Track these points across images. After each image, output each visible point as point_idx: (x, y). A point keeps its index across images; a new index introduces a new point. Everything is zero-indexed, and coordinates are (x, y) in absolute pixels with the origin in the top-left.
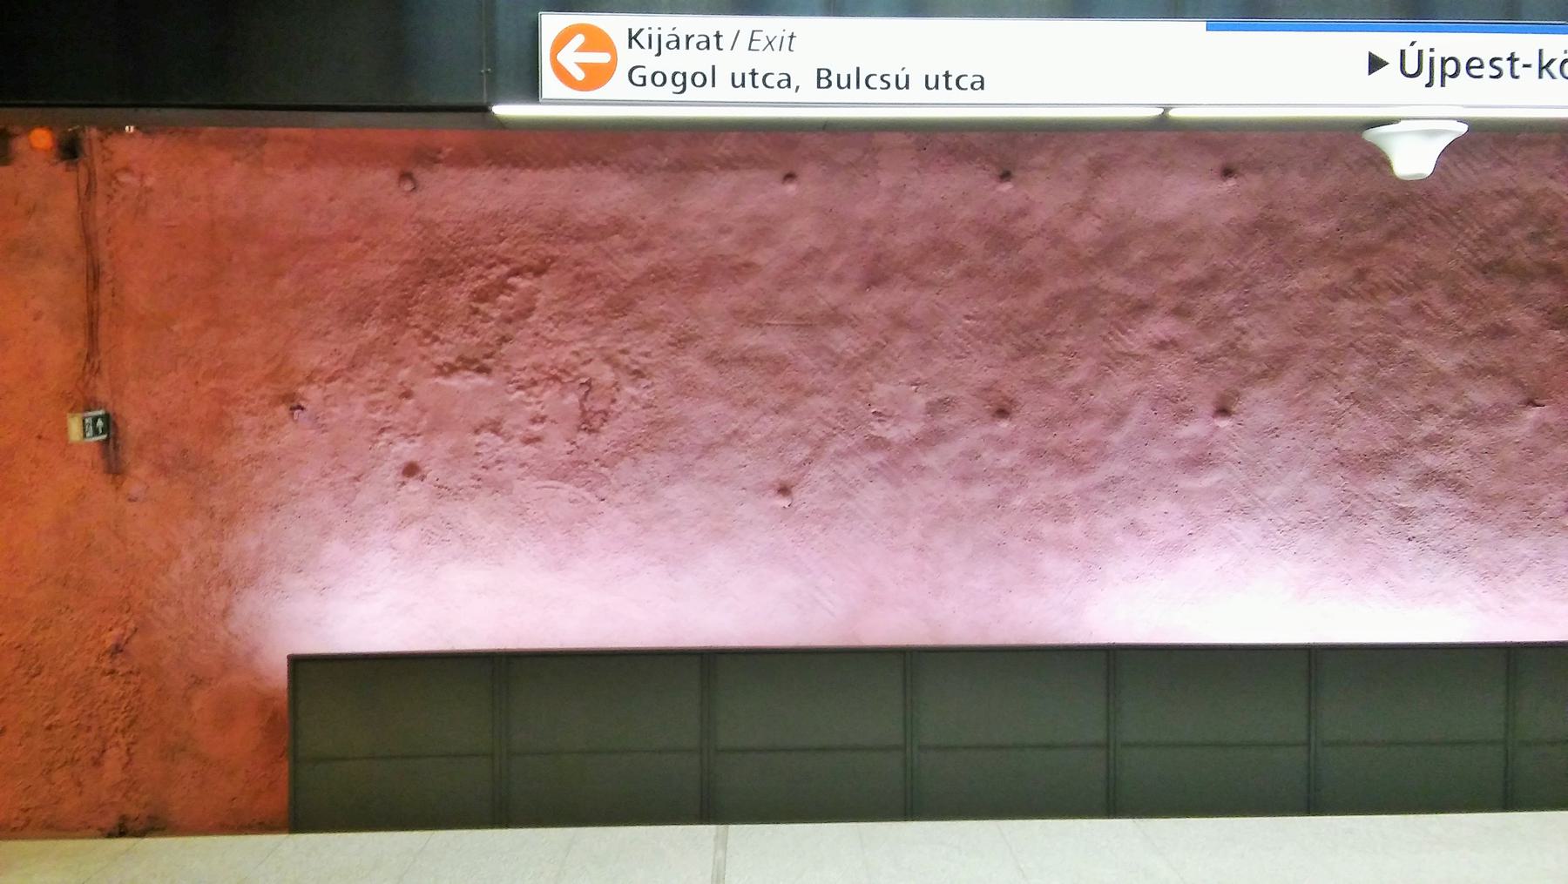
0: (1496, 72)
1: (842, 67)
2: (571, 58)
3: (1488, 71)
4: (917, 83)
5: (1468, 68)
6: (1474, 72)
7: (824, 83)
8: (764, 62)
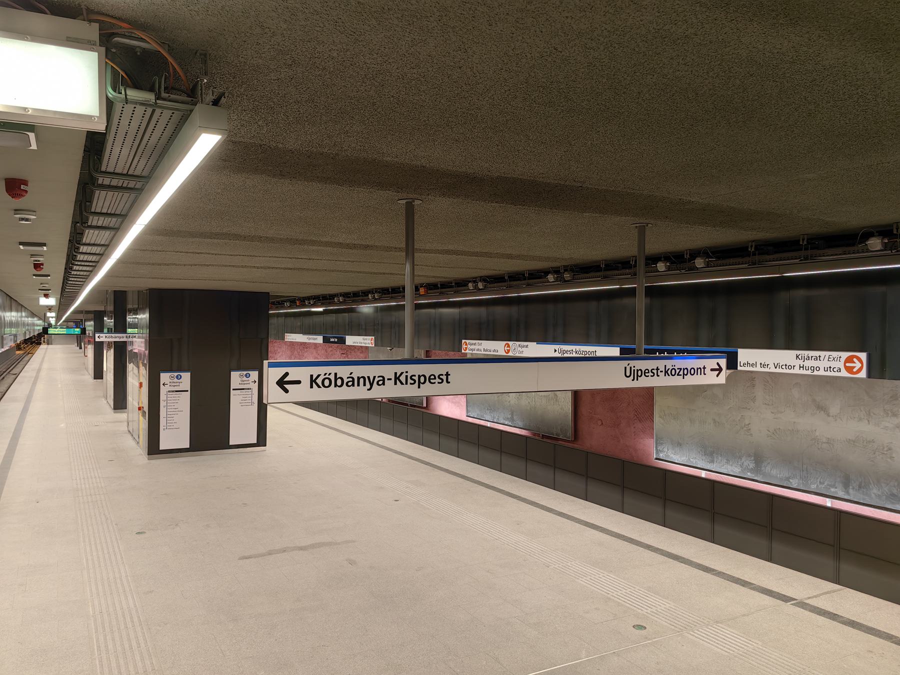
0: (440, 381)
3: (438, 380)
5: (430, 379)
6: (432, 381)
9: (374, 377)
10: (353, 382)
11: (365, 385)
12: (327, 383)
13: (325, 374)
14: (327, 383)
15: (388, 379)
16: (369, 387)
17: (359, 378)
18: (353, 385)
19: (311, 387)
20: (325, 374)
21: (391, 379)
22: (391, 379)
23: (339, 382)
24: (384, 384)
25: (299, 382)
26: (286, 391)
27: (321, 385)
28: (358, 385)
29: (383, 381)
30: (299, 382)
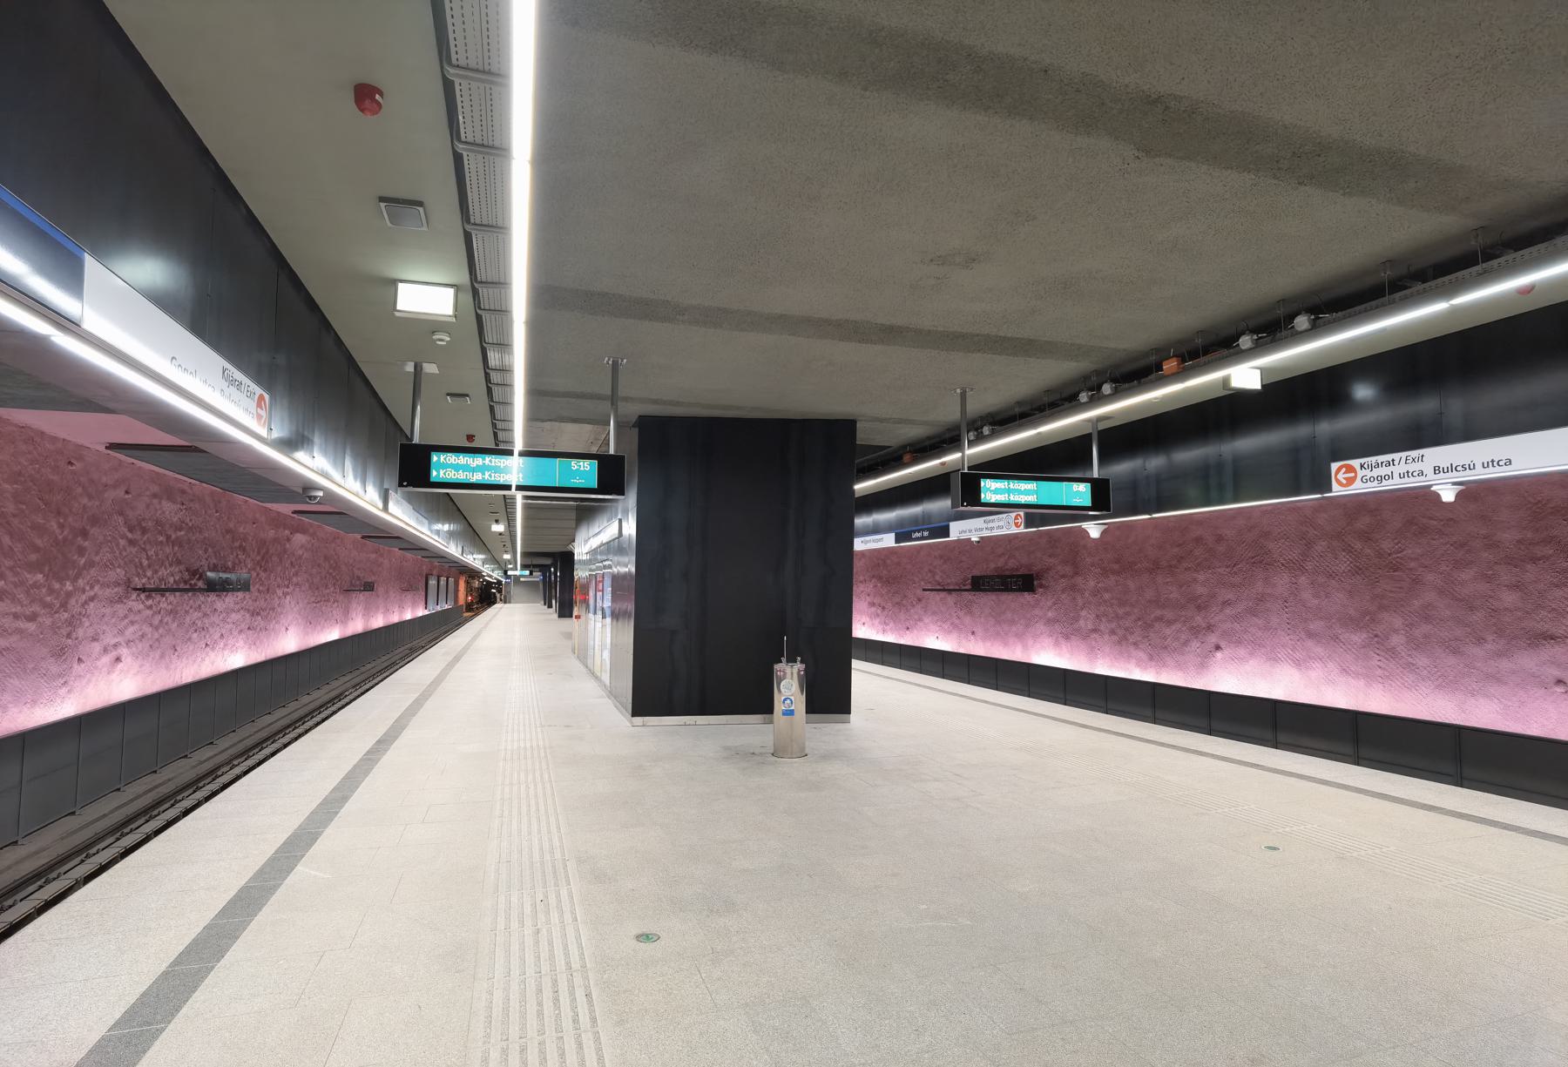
1: (1444, 464)
2: (1341, 476)
4: (1479, 466)
7: (1437, 472)
8: (1412, 467)
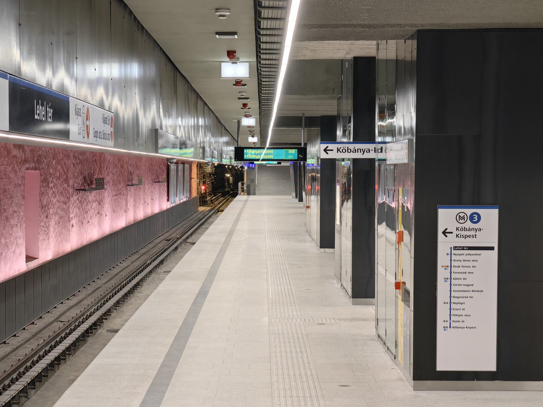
9: (365, 149)
10: (355, 151)
11: (361, 152)
12: (344, 151)
13: (343, 147)
14: (344, 151)
15: (371, 150)
16: (363, 153)
17: (358, 149)
18: (355, 152)
19: (338, 152)
20: (343, 147)
21: (373, 150)
22: (373, 150)
23: (349, 151)
24: (369, 152)
25: (332, 150)
26: (327, 153)
27: (342, 152)
28: (358, 152)
29: (369, 151)
30: (332, 150)
